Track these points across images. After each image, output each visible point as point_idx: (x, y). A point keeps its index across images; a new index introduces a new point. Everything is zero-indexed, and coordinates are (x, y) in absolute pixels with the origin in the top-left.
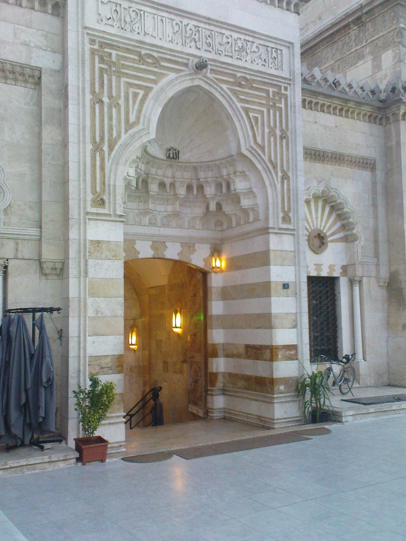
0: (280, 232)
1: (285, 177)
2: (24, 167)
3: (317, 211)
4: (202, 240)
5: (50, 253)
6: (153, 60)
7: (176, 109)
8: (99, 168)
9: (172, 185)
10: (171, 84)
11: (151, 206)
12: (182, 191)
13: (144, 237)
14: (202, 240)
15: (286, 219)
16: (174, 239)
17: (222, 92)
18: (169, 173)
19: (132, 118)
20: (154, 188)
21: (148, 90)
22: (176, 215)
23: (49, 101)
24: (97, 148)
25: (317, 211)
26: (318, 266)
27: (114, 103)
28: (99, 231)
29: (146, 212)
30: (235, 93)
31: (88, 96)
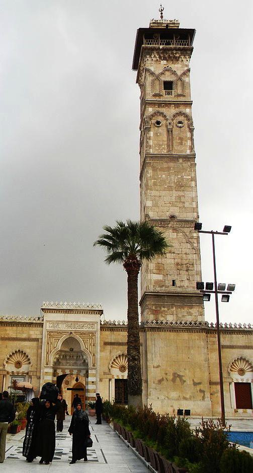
0: (92, 369)
1: (94, 355)
2: (35, 358)
3: (123, 360)
4: (84, 369)
5: (38, 374)
6: (60, 333)
7: (66, 342)
8: (47, 357)
9: (73, 356)
10: (64, 337)
11: (68, 362)
12: (75, 358)
13: (67, 369)
14: (84, 369)
15: (94, 366)
16: (75, 369)
17: (78, 337)
18: (72, 353)
19: (55, 346)
20: (68, 357)
21: (59, 340)
22: (76, 363)
23: (40, 344)
24: (47, 353)
25: (123, 360)
26: (123, 376)
27: (51, 343)
28: (46, 370)
29: (68, 363)
30: (80, 337)
31: (46, 343)
